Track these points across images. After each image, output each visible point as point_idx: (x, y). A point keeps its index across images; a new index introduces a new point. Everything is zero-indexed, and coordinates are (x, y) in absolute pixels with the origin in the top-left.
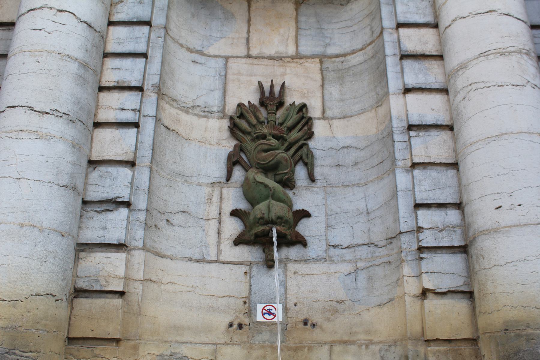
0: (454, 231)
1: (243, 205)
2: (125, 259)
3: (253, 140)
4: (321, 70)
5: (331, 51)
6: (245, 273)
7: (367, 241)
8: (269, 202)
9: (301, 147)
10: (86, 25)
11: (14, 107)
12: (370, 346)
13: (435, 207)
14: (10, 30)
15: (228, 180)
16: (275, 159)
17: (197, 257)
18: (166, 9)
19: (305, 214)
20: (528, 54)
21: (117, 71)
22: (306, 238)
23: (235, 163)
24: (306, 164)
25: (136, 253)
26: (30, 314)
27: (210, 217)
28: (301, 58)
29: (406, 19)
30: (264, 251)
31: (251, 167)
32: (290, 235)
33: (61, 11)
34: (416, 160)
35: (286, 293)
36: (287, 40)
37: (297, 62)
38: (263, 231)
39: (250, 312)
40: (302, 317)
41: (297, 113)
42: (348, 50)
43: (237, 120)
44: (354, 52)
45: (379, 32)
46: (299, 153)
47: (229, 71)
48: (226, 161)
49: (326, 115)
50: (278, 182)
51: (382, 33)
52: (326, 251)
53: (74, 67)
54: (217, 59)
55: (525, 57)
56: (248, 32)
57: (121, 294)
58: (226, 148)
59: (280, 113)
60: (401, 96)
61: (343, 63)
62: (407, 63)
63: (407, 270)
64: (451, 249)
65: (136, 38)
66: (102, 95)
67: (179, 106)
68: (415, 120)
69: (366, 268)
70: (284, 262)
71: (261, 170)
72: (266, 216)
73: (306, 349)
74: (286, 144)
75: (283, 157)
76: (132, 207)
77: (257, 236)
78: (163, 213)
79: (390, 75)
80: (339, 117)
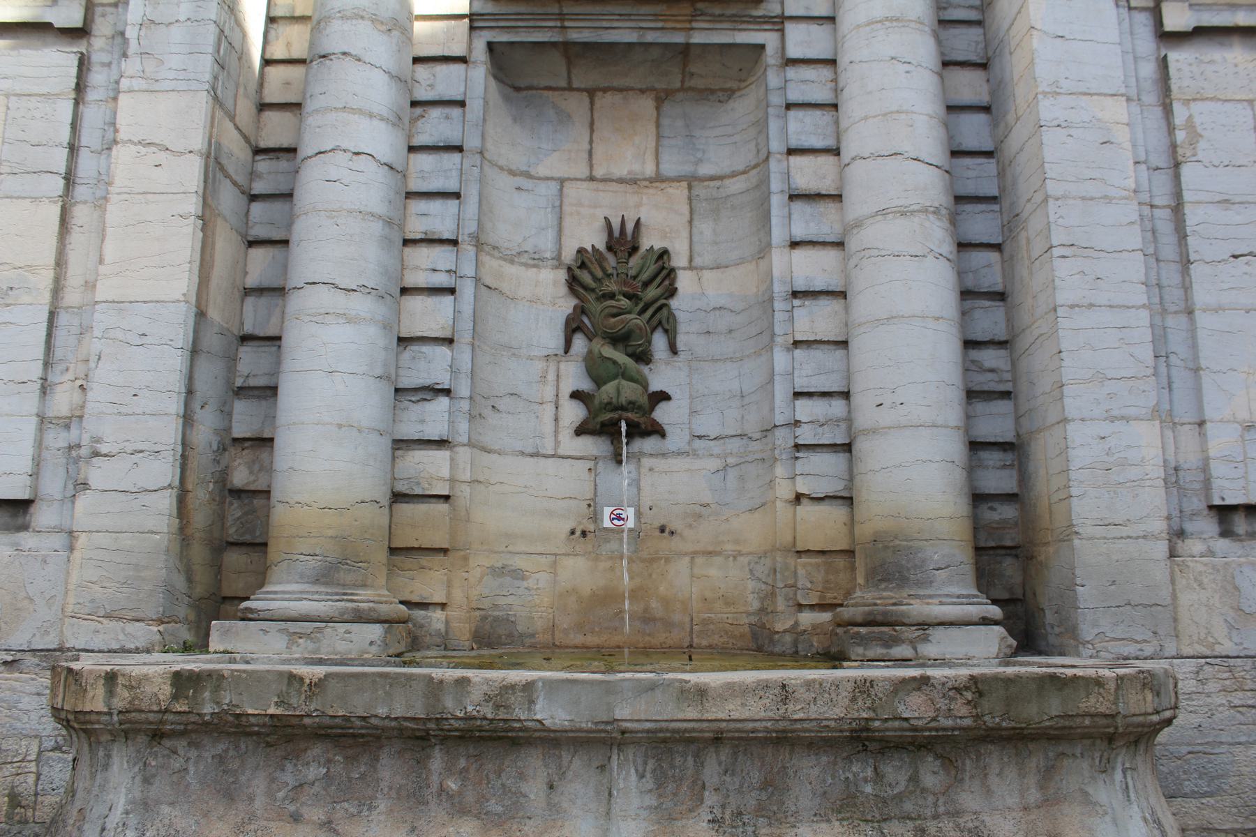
0: (838, 426)
1: (586, 385)
2: (448, 458)
3: (599, 299)
4: (690, 199)
5: (705, 170)
6: (590, 469)
7: (739, 432)
8: (619, 383)
9: (660, 308)
10: (386, 167)
11: (314, 283)
12: (738, 558)
13: (818, 396)
14: (278, 158)
15: (566, 352)
16: (627, 327)
17: (530, 450)
18: (481, 124)
19: (663, 396)
20: (936, 212)
21: (424, 218)
22: (665, 427)
23: (574, 331)
24: (666, 331)
25: (461, 450)
26: (356, 523)
27: (545, 400)
28: (663, 181)
29: (799, 143)
30: (612, 443)
31: (595, 336)
32: (645, 423)
33: (357, 154)
34: (799, 338)
35: (639, 494)
36: (644, 154)
37: (657, 187)
38: (611, 419)
39: (596, 517)
40: (657, 524)
41: (656, 262)
42: (727, 171)
43: (578, 272)
44: (734, 175)
45: (766, 155)
46: (658, 316)
47: (566, 201)
48: (563, 327)
49: (694, 264)
50: (629, 355)
51: (767, 158)
52: (689, 443)
53: (377, 227)
54: (549, 182)
55: (931, 217)
56: (591, 142)
57: (446, 498)
58: (563, 308)
59: (634, 261)
60: (788, 249)
61: (721, 190)
62: (798, 206)
63: (780, 471)
64: (833, 447)
65: (445, 171)
66: (408, 250)
67: (501, 255)
68: (800, 286)
69: (737, 465)
70: (637, 457)
71: (608, 340)
72: (614, 400)
73: (663, 561)
74: (641, 305)
75: (637, 325)
76: (452, 395)
77: (603, 425)
78: (487, 398)
79: (774, 221)
80: (711, 266)
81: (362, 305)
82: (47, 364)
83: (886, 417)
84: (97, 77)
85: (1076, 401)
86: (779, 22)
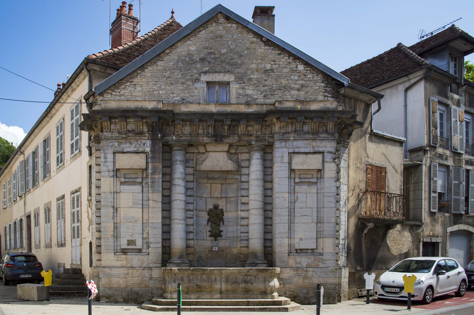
53: (184, 210)
57: (193, 247)
81: (183, 222)
82: (142, 231)
83: (253, 237)
84: (144, 189)
85: (277, 236)
86: (241, 175)
